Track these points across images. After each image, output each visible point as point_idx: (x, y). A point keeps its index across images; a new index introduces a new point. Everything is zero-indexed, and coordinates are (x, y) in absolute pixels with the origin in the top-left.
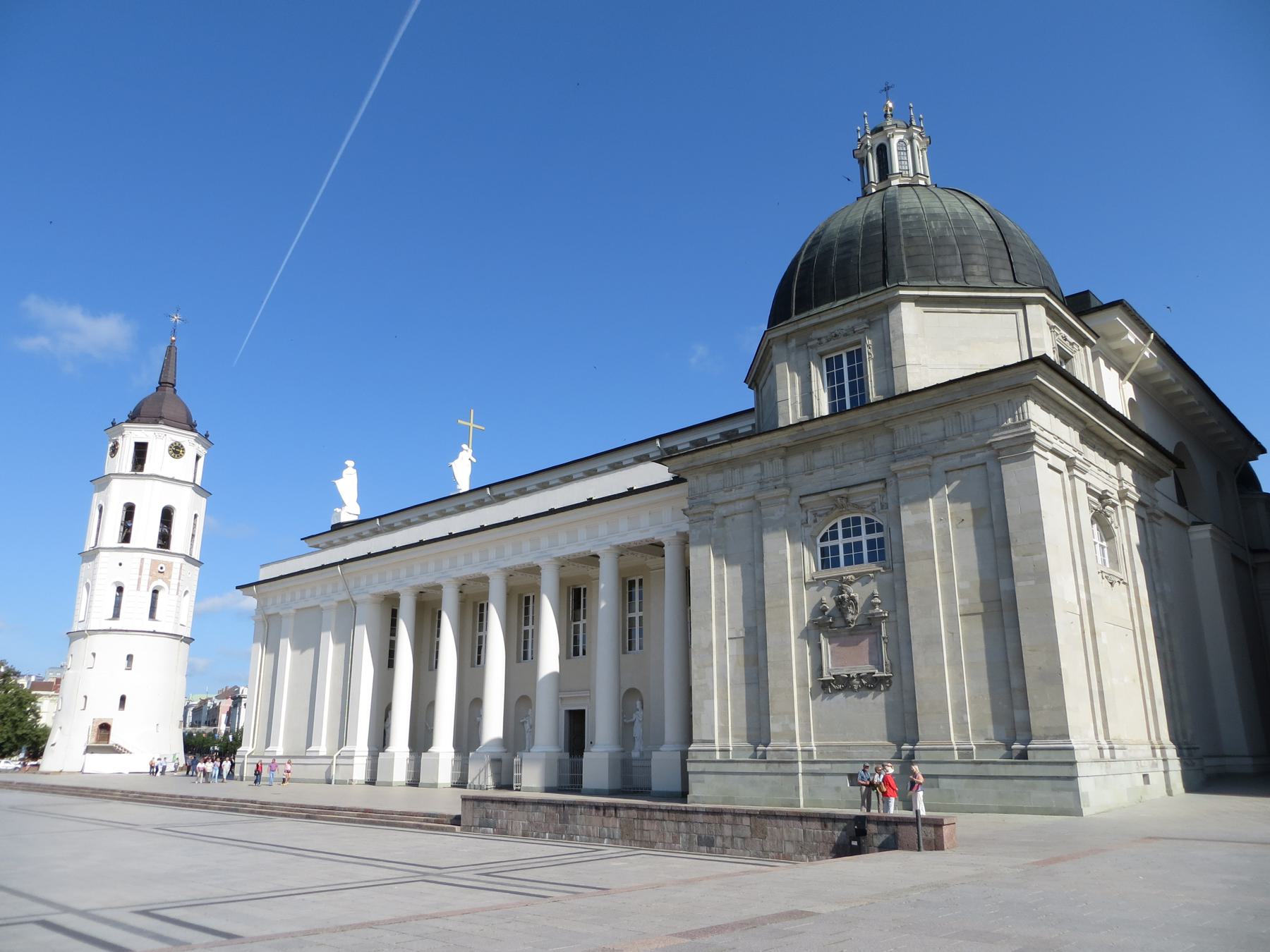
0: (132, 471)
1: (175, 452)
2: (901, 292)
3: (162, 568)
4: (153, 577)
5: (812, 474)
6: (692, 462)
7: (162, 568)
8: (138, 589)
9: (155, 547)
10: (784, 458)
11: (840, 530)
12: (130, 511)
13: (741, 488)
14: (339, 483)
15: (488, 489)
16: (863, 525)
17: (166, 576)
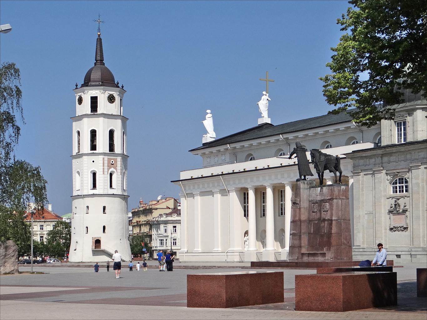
0: (91, 112)
1: (111, 100)
2: (417, 107)
3: (112, 162)
4: (109, 167)
5: (389, 163)
6: (353, 156)
7: (112, 162)
8: (104, 174)
9: (108, 152)
10: (382, 157)
11: (398, 181)
12: (93, 133)
13: (369, 166)
14: (204, 122)
15: (281, 135)
16: (404, 181)
17: (115, 166)
